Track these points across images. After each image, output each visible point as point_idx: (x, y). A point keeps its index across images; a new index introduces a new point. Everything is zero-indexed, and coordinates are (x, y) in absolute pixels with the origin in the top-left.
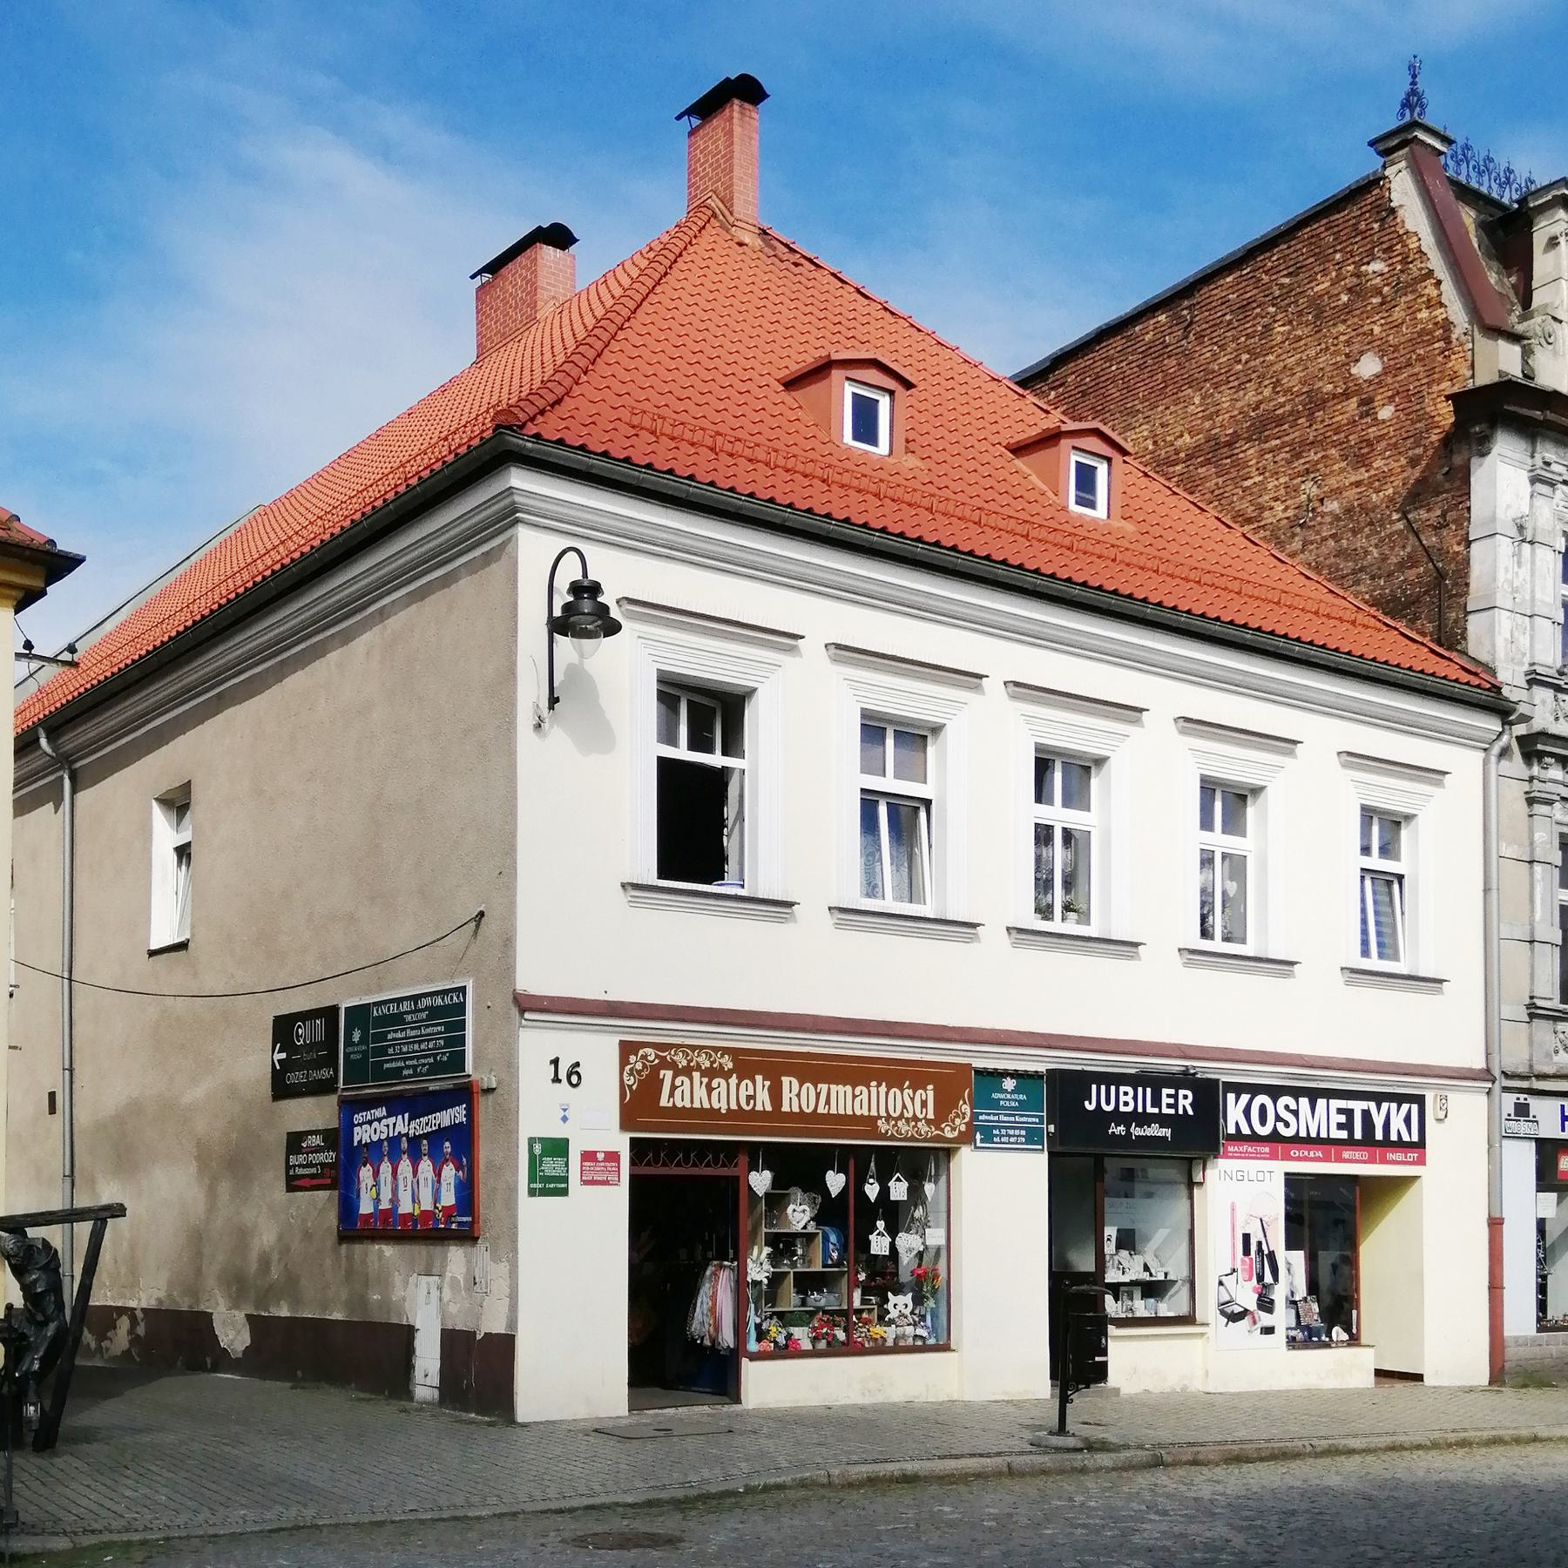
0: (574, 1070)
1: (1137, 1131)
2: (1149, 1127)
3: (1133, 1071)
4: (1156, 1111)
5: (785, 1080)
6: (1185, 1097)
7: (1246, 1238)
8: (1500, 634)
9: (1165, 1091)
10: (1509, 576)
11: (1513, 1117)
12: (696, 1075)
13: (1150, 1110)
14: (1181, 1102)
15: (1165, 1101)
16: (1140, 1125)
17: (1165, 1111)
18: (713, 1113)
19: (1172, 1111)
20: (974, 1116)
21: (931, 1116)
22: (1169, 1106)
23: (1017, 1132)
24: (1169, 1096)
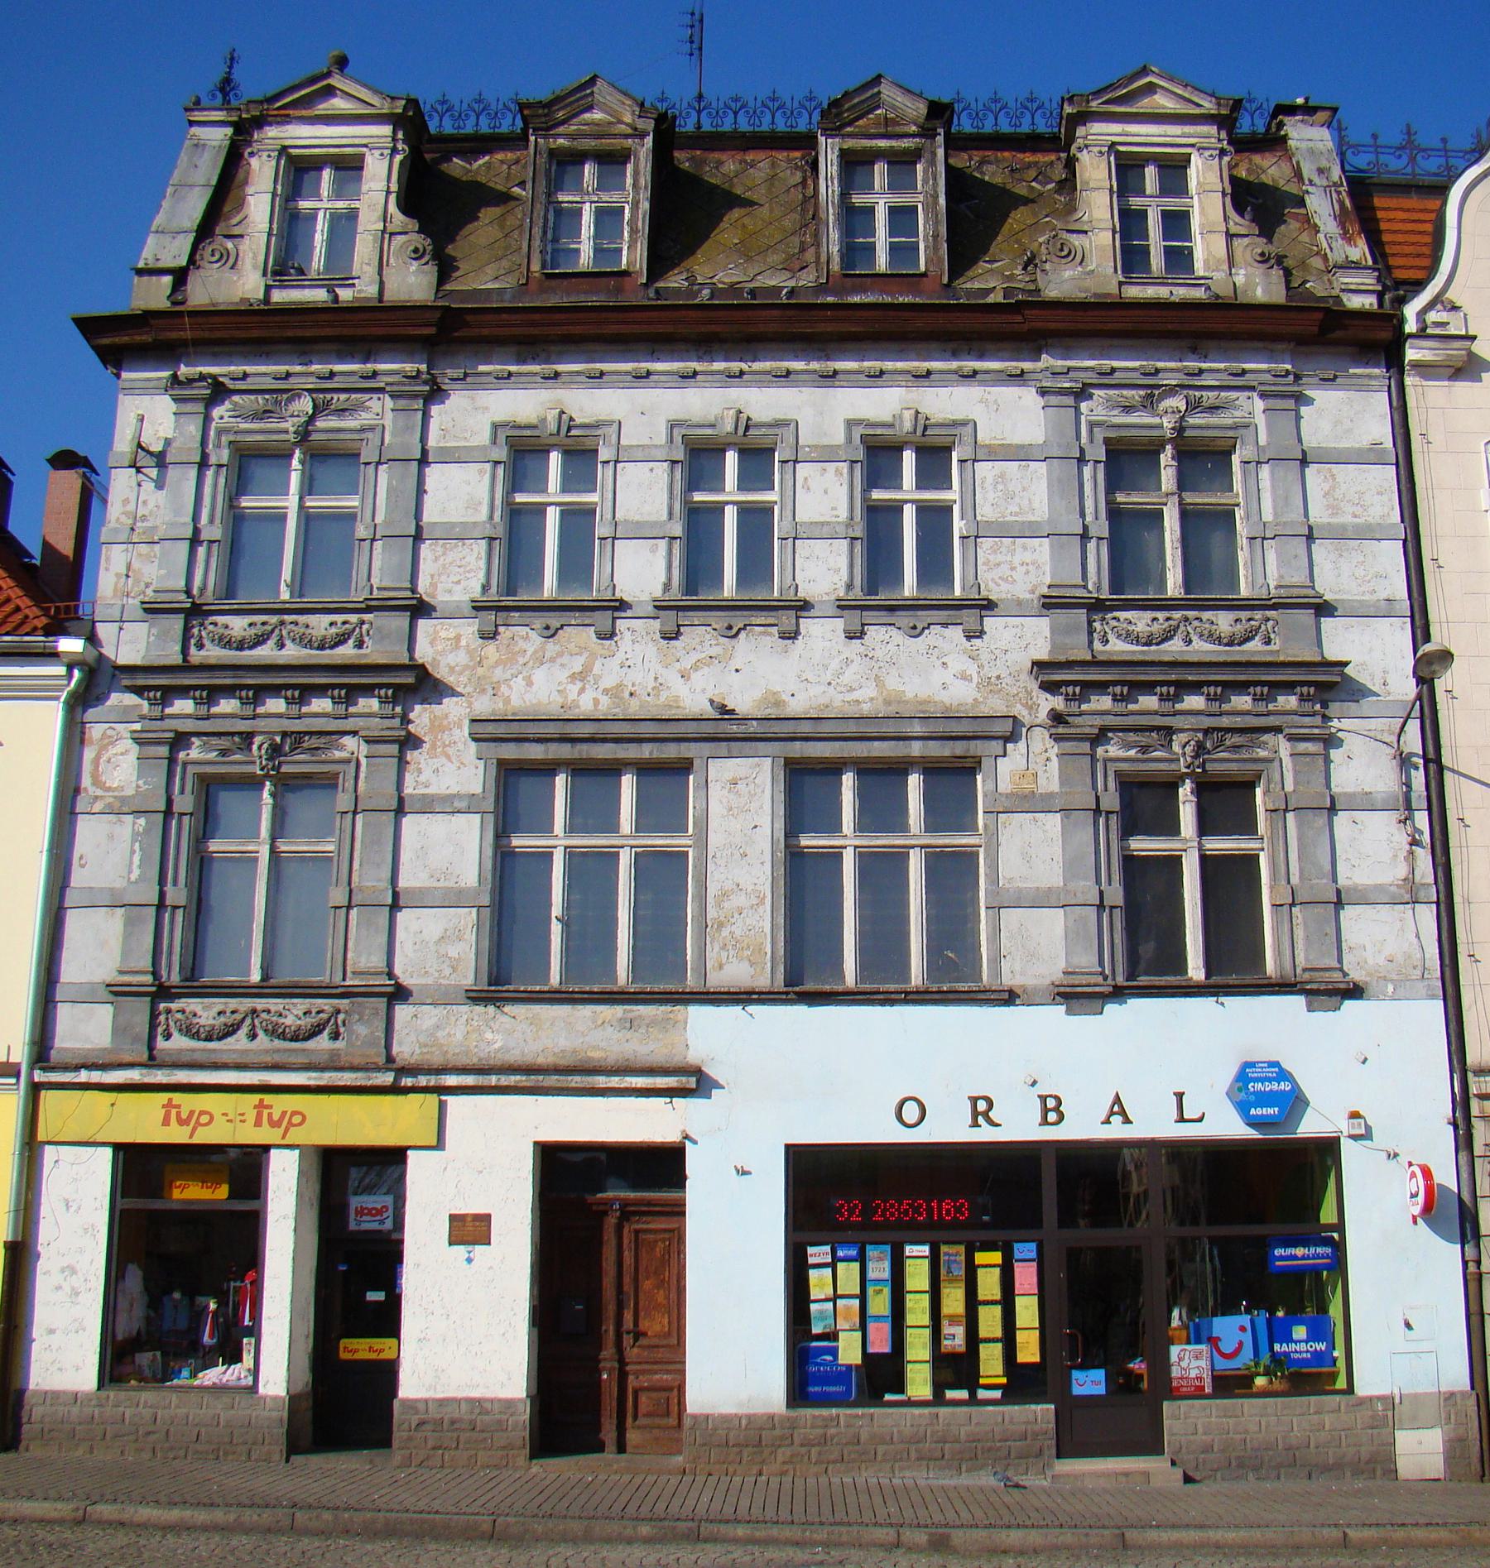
8: (107, 569)
10: (131, 507)
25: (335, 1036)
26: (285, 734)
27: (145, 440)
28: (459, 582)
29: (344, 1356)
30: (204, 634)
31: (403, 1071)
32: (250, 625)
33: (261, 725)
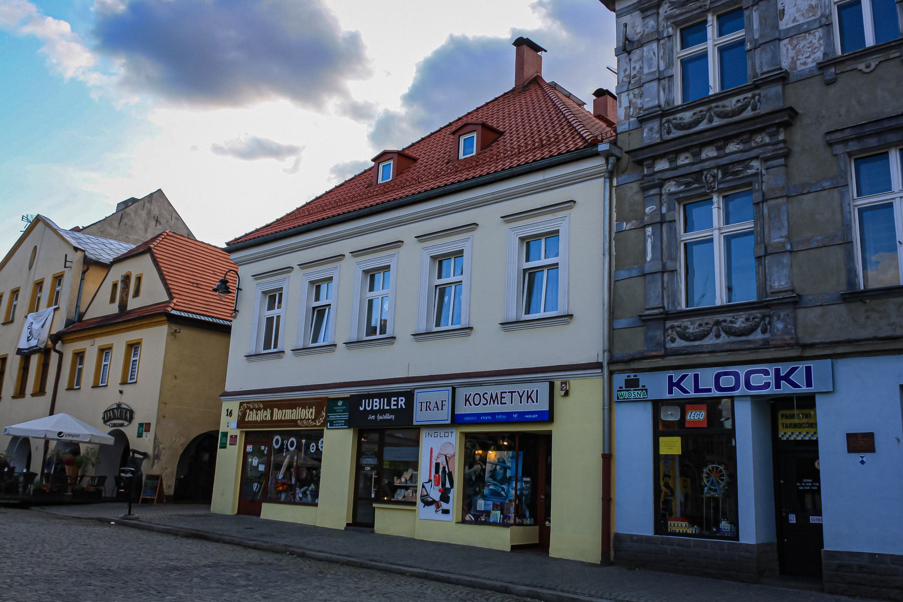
0: (231, 412)
1: (380, 417)
2: (385, 415)
3: (409, 390)
4: (388, 408)
5: (275, 409)
6: (376, 402)
7: (437, 465)
9: (393, 399)
10: (628, 72)
11: (624, 389)
12: (254, 410)
13: (386, 408)
14: (400, 402)
15: (393, 403)
16: (381, 415)
17: (393, 407)
18: (256, 422)
19: (396, 407)
20: (327, 416)
21: (313, 418)
22: (394, 405)
23: (341, 421)
24: (394, 401)
25: (764, 331)
26: (718, 167)
27: (630, 37)
28: (809, 57)
29: (811, 522)
30: (670, 125)
31: (805, 346)
32: (694, 114)
33: (706, 165)
